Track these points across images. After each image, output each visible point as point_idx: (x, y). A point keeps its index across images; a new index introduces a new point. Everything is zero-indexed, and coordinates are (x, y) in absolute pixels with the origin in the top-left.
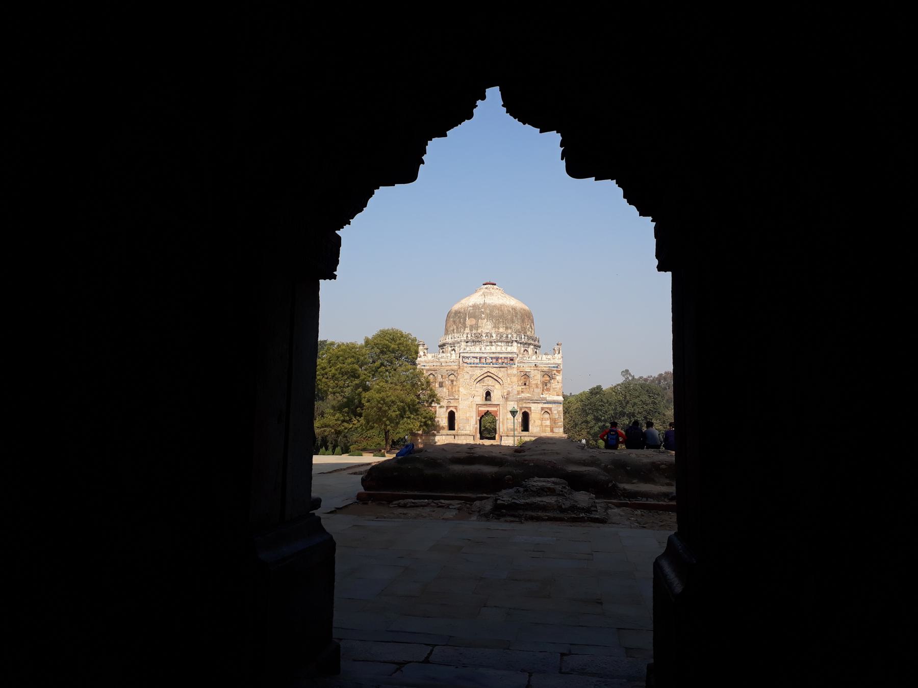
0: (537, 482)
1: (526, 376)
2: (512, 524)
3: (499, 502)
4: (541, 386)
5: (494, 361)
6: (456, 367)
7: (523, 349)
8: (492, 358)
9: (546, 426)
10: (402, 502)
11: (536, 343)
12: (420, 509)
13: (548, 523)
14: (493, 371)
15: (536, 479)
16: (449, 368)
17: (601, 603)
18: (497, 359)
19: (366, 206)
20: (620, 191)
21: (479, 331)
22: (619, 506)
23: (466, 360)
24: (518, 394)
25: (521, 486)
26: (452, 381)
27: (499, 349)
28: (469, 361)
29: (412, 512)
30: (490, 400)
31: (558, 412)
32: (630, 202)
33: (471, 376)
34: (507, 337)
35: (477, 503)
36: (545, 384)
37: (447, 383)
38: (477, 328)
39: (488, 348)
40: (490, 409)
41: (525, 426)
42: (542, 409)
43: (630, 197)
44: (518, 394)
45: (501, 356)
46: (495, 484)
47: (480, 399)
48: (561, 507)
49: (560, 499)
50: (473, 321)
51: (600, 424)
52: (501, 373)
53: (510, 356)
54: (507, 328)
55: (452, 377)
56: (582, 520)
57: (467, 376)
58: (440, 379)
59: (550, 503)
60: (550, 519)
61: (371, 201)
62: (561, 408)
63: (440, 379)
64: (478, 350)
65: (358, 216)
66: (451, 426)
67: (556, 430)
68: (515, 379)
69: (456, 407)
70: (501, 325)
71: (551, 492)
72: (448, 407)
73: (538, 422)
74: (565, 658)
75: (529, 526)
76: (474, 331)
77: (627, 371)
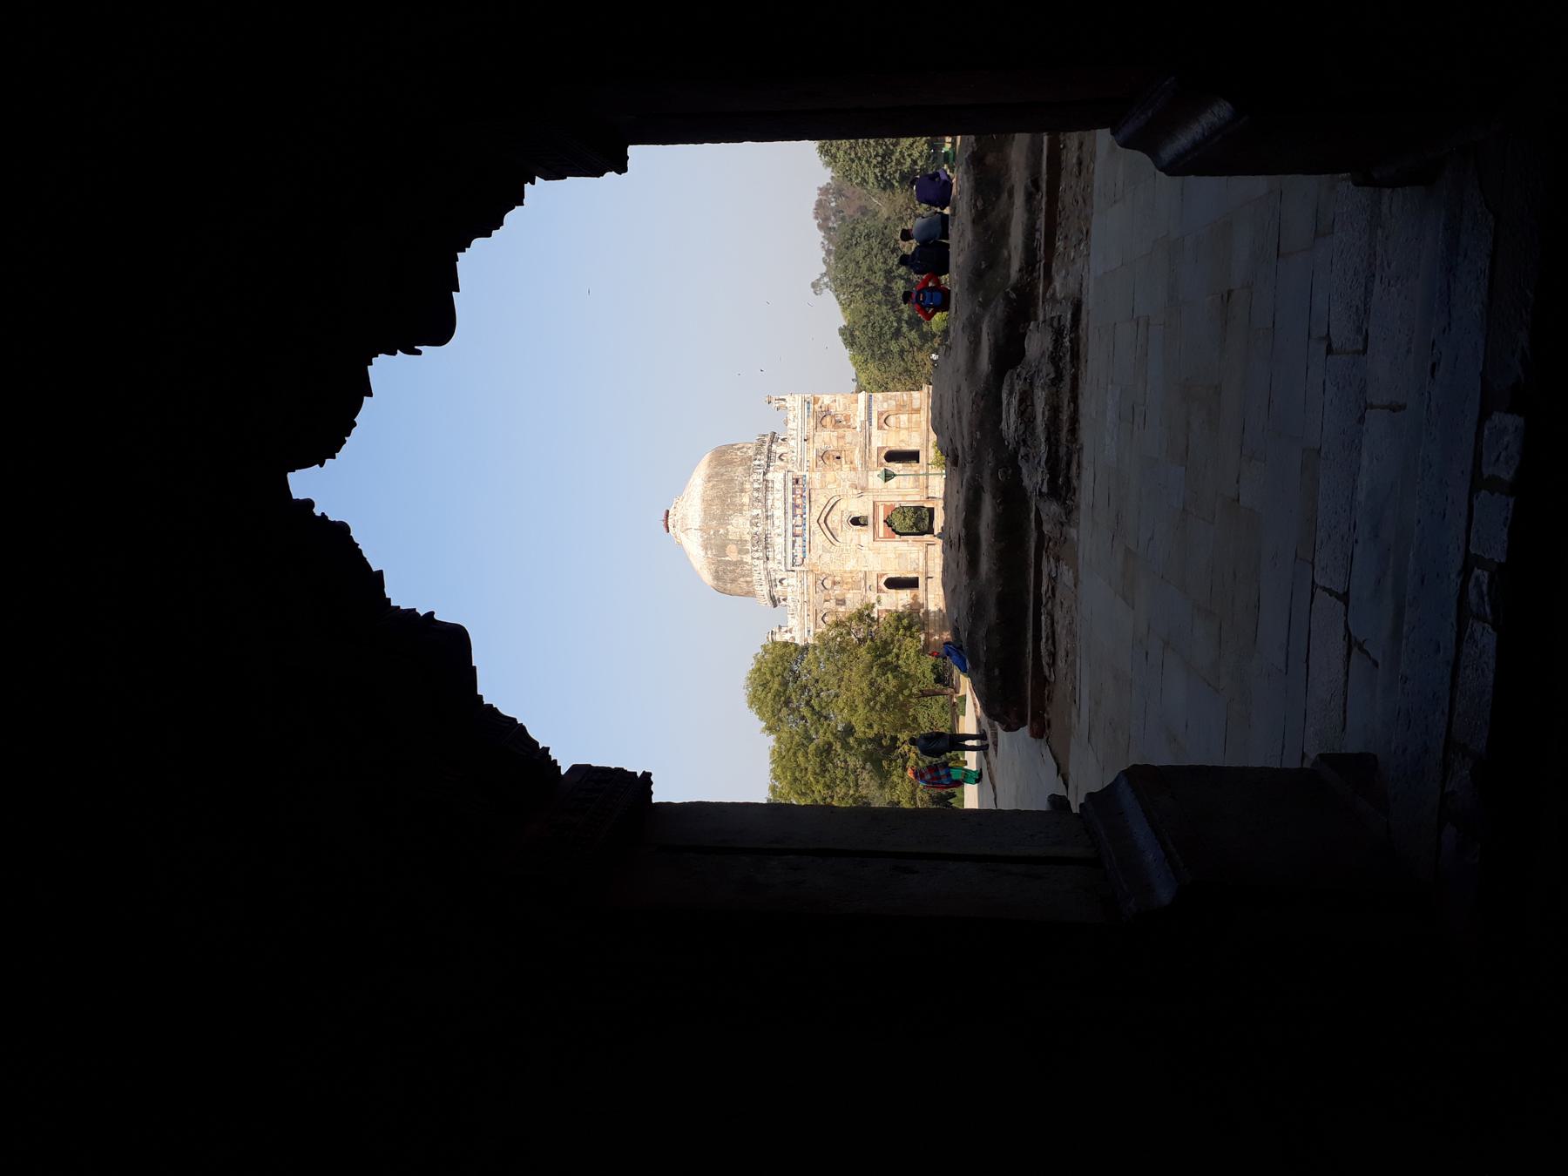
0: (1010, 423)
1: (823, 456)
2: (1085, 463)
3: (1045, 489)
5: (799, 511)
6: (811, 578)
7: (778, 463)
8: (794, 516)
9: (909, 421)
10: (1045, 660)
11: (767, 439)
12: (1058, 628)
13: (1081, 402)
14: (816, 513)
15: (1004, 425)
16: (812, 590)
17: (1230, 293)
18: (795, 506)
19: (514, 720)
20: (477, 243)
21: (748, 538)
22: (1049, 279)
23: (799, 561)
24: (855, 469)
25: (1016, 452)
26: (834, 583)
27: (779, 504)
28: (800, 555)
29: (1063, 643)
30: (866, 518)
31: (885, 400)
32: (498, 223)
33: (825, 550)
34: (757, 490)
35: (1046, 528)
36: (837, 423)
37: (837, 591)
38: (742, 542)
39: (777, 522)
40: (881, 518)
41: (911, 456)
42: (880, 428)
43: (489, 223)
44: (855, 469)
46: (1012, 498)
47: (865, 535)
48: (1053, 380)
49: (1038, 383)
50: (732, 548)
51: (905, 328)
52: (820, 500)
53: (790, 484)
54: (742, 491)
55: (828, 584)
56: (1075, 342)
57: (826, 558)
58: (831, 605)
59: (1046, 399)
60: (1074, 399)
61: (506, 711)
62: (879, 396)
63: (831, 605)
64: (780, 540)
65: (533, 733)
66: (911, 583)
67: (916, 404)
68: (830, 476)
69: (879, 576)
70: (737, 500)
71: (1026, 399)
72: (879, 590)
73: (904, 434)
74: (1334, 346)
75: (1086, 435)
76: (749, 546)
77: (814, 285)
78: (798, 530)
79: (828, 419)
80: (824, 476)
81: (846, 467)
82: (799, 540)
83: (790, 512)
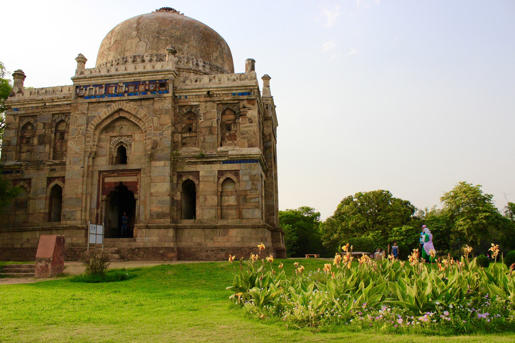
1: (192, 113)
4: (217, 130)
5: (132, 89)
8: (127, 84)
9: (229, 207)
18: (136, 84)
24: (175, 146)
28: (87, 93)
31: (252, 178)
45: (143, 79)
47: (103, 163)
53: (160, 77)
55: (62, 127)
57: (82, 120)
58: (40, 129)
67: (247, 213)
68: (167, 119)
69: (63, 179)
73: (213, 200)
78: (113, 90)
79: (232, 117)
80: (167, 112)
81: (178, 138)
82: (103, 91)
83: (132, 79)
